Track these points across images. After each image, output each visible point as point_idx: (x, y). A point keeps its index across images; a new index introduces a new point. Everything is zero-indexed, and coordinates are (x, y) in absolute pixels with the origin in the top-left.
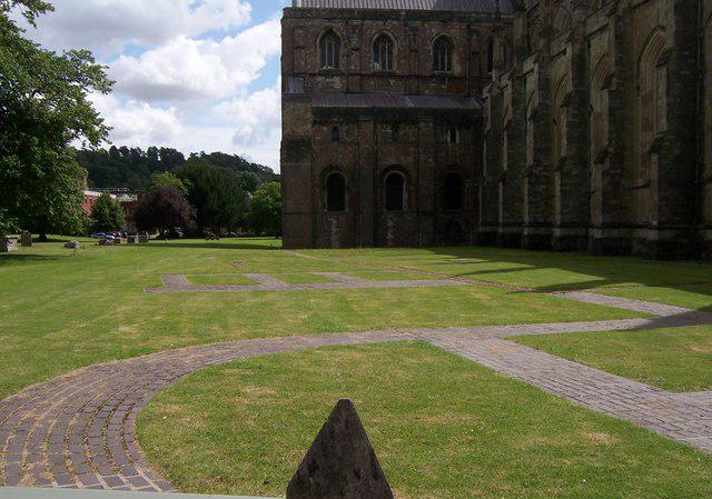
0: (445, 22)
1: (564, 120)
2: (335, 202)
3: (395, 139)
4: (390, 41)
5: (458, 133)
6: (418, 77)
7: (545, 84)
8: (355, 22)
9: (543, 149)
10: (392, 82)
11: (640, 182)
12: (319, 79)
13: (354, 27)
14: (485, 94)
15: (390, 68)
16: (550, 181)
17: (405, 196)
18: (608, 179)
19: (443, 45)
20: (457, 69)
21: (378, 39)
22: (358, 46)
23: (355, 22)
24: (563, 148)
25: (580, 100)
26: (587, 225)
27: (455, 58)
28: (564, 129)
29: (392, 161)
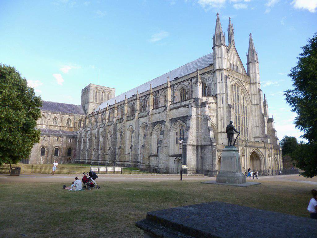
0: (70, 116)
4: (57, 118)
5: (71, 140)
7: (91, 134)
8: (50, 114)
9: (90, 146)
10: (57, 127)
11: (107, 154)
12: (40, 125)
13: (49, 115)
14: (78, 132)
15: (57, 124)
16: (91, 152)
17: (59, 153)
18: (102, 153)
19: (69, 120)
20: (72, 126)
21: (54, 118)
23: (50, 114)
24: (94, 146)
25: (98, 139)
26: (98, 160)
27: (71, 123)
28: (95, 143)
29: (57, 145)
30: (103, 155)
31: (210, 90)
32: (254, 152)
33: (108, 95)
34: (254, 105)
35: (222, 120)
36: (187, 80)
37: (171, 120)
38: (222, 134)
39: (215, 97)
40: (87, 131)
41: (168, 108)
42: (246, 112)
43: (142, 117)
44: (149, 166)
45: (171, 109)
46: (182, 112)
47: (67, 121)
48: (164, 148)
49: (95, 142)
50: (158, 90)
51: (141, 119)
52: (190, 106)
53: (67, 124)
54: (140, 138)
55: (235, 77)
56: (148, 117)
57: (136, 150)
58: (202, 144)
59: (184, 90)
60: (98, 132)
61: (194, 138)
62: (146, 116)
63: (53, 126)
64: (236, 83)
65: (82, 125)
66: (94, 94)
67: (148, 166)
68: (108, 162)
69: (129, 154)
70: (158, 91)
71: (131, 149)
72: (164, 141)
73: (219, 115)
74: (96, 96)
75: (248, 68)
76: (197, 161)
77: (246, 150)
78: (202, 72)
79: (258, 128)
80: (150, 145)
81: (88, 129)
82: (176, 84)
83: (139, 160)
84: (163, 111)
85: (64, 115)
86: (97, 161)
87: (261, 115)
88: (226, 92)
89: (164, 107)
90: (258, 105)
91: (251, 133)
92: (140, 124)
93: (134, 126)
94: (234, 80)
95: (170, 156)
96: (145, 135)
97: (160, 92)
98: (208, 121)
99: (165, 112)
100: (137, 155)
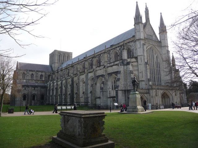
0: (42, 73)
1: (59, 90)
2: (24, 99)
3: (34, 89)
6: (38, 80)
7: (57, 85)
9: (57, 93)
16: (58, 97)
17: (35, 98)
19: (42, 76)
20: (43, 79)
24: (59, 93)
25: (61, 88)
26: (62, 102)
27: (43, 78)
29: (34, 93)
30: (66, 99)
31: (133, 53)
32: (165, 93)
33: (68, 57)
36: (119, 47)
37: (109, 74)
39: (136, 58)
40: (54, 83)
41: (106, 67)
42: (159, 66)
43: (90, 72)
44: (96, 105)
45: (108, 67)
46: (115, 69)
48: (104, 93)
49: (59, 90)
51: (89, 74)
52: (119, 65)
54: (89, 86)
55: (150, 43)
56: (93, 72)
57: (87, 94)
58: (128, 89)
59: (117, 53)
60: (61, 83)
61: (123, 85)
62: (92, 72)
65: (50, 79)
66: (58, 57)
67: (95, 105)
68: (69, 103)
69: (82, 97)
70: (100, 55)
71: (83, 94)
72: (104, 88)
73: (139, 70)
74: (59, 58)
75: (160, 36)
76: (125, 100)
77: (159, 92)
78: (128, 41)
80: (95, 91)
81: (55, 81)
82: (112, 49)
83: (89, 101)
84: (103, 68)
86: (61, 103)
88: (143, 54)
89: (104, 66)
92: (89, 77)
93: (85, 79)
95: (108, 98)
96: (92, 85)
97: (101, 55)
99: (104, 69)
100: (88, 98)
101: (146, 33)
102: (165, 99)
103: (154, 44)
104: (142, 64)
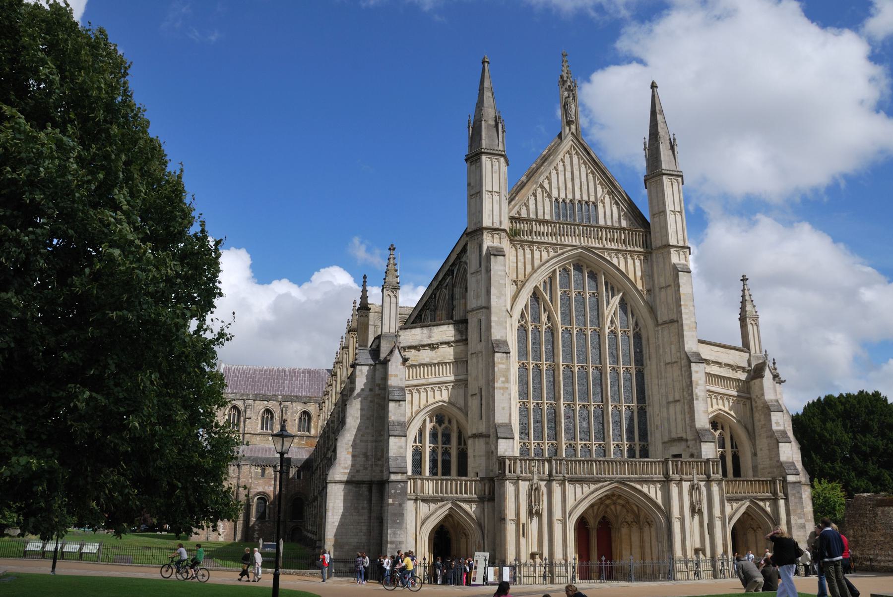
0: (305, 403)
5: (302, 473)
22: (250, 416)
29: (260, 489)
34: (665, 323)
35: (479, 395)
38: (477, 440)
47: (300, 419)
50: (420, 311)
53: (300, 426)
63: (259, 434)
64: (579, 260)
79: (678, 407)
85: (288, 404)
87: (685, 357)
90: (676, 324)
91: (657, 426)
94: (560, 252)
98: (392, 405)
101: (550, 196)
102: (641, 529)
103: (594, 244)
104: (481, 352)
